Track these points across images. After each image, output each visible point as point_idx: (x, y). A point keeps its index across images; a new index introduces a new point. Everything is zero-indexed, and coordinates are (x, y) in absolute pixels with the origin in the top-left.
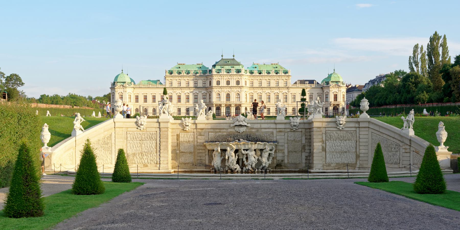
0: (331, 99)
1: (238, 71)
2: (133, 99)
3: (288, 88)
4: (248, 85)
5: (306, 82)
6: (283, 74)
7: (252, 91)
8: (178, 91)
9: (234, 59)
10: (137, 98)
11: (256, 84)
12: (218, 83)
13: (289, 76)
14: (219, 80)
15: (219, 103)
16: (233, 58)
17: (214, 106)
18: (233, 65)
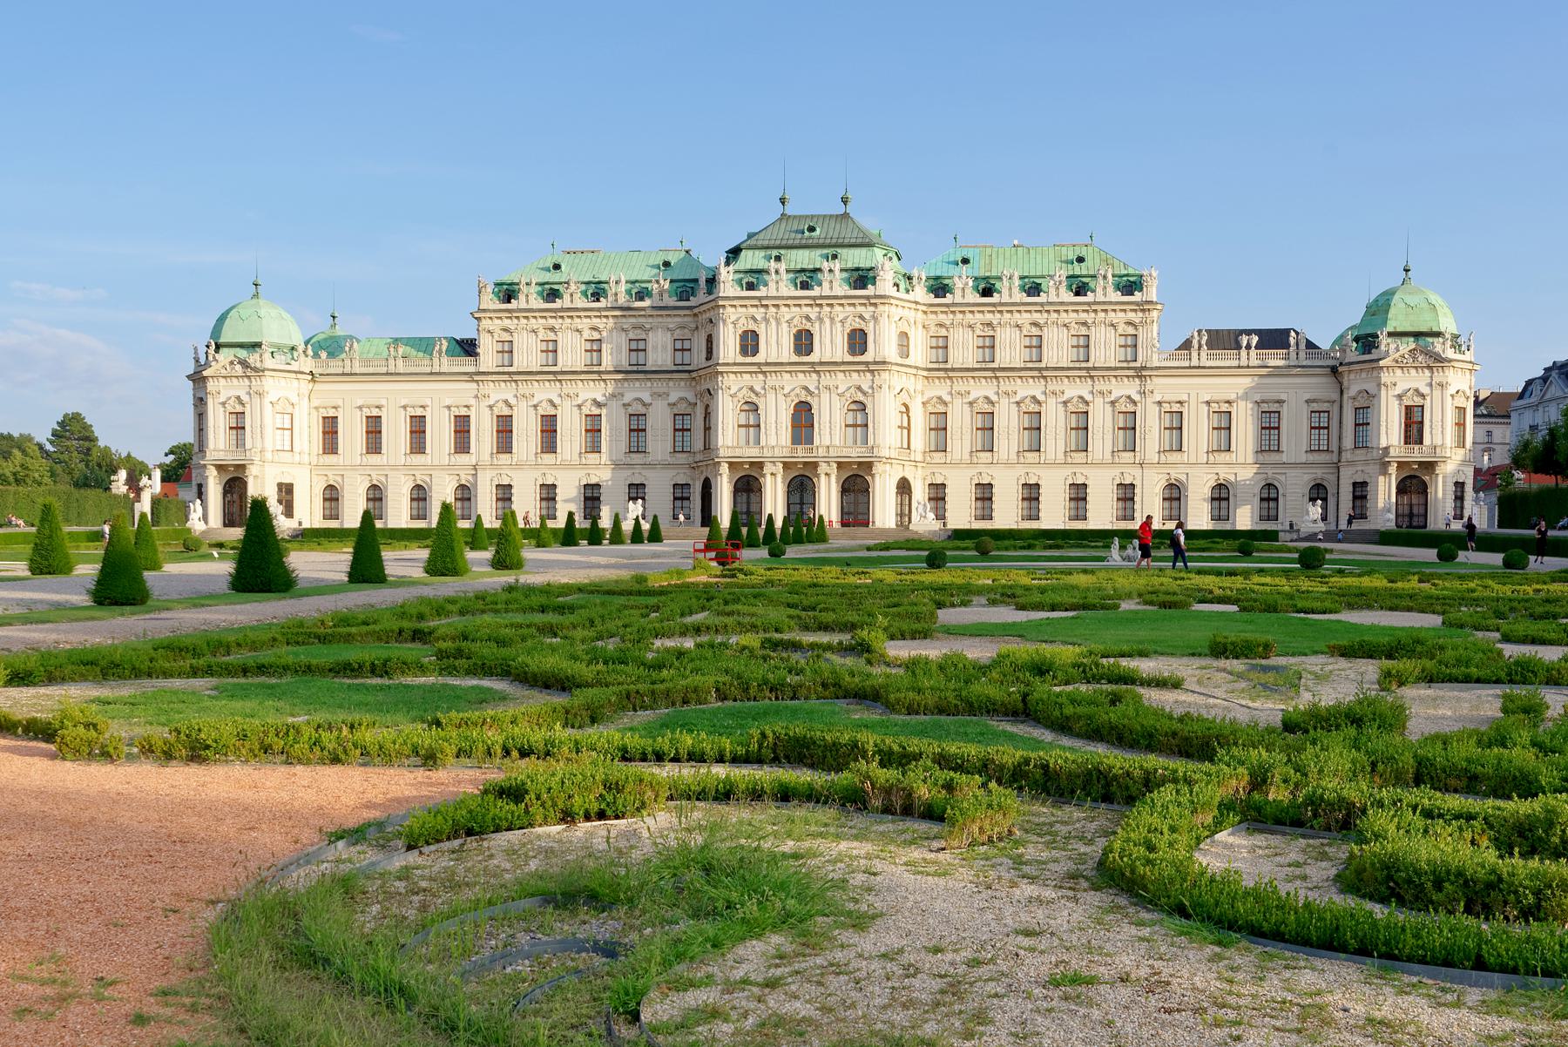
0: (1390, 432)
1: (862, 278)
2: (309, 436)
3: (1141, 373)
4: (920, 353)
5: (1244, 340)
6: (1116, 296)
7: (941, 389)
8: (544, 392)
9: (845, 216)
10: (330, 429)
11: (964, 351)
12: (750, 343)
13: (1144, 307)
14: (752, 326)
15: (752, 453)
16: (840, 209)
17: (724, 469)
18: (833, 248)
